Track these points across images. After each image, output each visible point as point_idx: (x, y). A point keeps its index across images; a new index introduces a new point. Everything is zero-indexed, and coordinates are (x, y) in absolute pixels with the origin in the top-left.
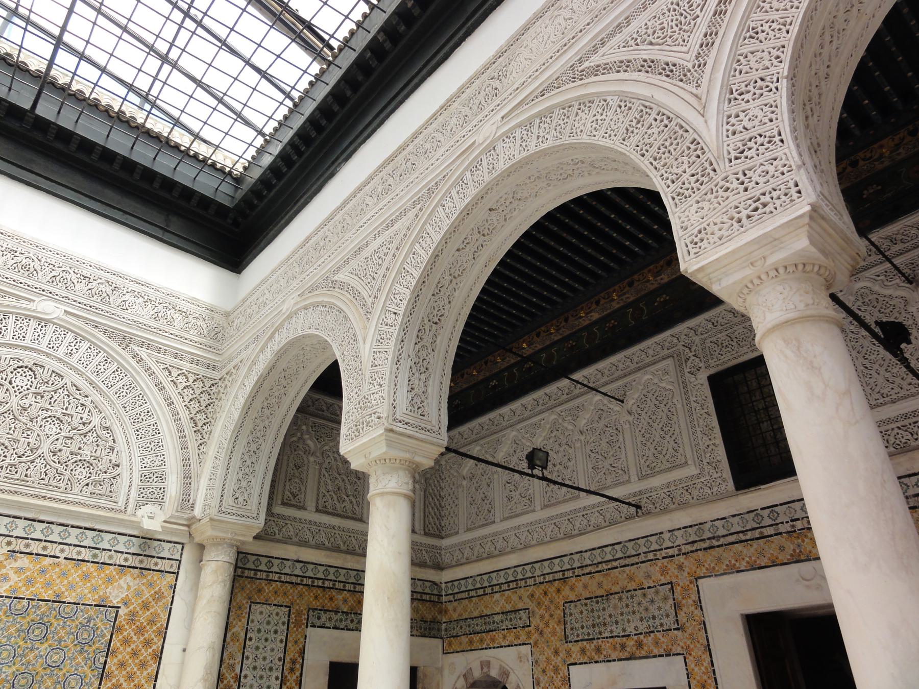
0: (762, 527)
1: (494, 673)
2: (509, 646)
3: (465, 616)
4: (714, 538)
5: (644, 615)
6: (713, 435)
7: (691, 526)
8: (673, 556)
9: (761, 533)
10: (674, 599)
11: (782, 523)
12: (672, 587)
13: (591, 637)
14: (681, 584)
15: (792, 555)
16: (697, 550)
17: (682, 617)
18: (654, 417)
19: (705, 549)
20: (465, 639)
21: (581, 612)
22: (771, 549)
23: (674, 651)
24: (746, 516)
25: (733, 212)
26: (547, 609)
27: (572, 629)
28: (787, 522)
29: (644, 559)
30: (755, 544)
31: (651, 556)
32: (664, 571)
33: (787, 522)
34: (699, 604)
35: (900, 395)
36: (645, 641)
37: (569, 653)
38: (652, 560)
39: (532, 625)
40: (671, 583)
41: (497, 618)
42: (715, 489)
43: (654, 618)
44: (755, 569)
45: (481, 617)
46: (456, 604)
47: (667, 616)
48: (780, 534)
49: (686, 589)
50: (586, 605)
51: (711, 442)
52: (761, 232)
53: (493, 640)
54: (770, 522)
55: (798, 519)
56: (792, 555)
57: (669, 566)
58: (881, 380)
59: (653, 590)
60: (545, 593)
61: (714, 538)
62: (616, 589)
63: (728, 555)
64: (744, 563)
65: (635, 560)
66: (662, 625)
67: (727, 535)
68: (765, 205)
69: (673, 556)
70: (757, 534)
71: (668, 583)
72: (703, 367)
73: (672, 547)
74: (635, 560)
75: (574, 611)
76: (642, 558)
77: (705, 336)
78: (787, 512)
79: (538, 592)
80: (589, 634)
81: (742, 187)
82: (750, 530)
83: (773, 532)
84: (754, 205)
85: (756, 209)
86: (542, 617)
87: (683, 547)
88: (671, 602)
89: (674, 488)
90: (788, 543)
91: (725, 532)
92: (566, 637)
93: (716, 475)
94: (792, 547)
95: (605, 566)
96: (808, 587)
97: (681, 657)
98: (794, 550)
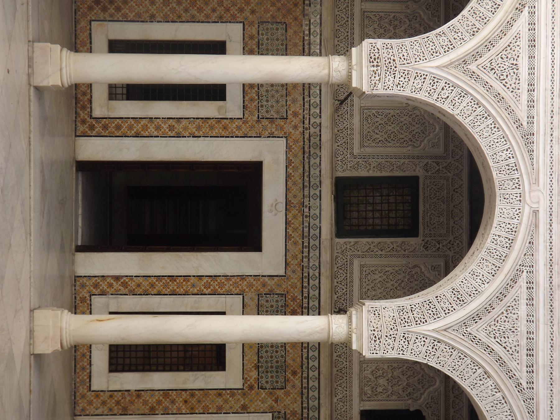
0: (310, 188)
4: (310, 155)
5: (270, 93)
6: (376, 170)
7: (320, 140)
8: (304, 124)
9: (306, 187)
10: (277, 118)
11: (309, 201)
12: (284, 119)
13: (260, 46)
14: (285, 126)
15: (291, 201)
16: (304, 142)
17: (265, 122)
18: (404, 128)
19: (304, 147)
21: (278, 40)
22: (295, 190)
23: (246, 112)
24: (318, 179)
25: (379, 329)
27: (267, 29)
28: (309, 204)
29: (306, 100)
30: (300, 181)
31: (307, 106)
32: (295, 114)
33: (309, 204)
34: (271, 136)
35: (364, 284)
36: (254, 91)
37: (251, 24)
38: (304, 106)
40: (287, 119)
42: (340, 163)
43: (267, 101)
44: (286, 178)
47: (267, 112)
48: (304, 198)
49: (282, 128)
50: (282, 45)
51: (372, 167)
52: (364, 337)
54: (311, 194)
55: (309, 210)
56: (291, 201)
57: (298, 119)
58: (376, 277)
59: (285, 103)
61: (310, 155)
63: (297, 162)
64: (291, 172)
65: (306, 93)
66: (262, 106)
67: (309, 164)
68: (375, 341)
69: (304, 124)
70: (306, 184)
71: (287, 116)
72: (427, 174)
73: (309, 124)
74: (306, 93)
75: (280, 32)
76: (307, 99)
77: (450, 181)
78: (315, 205)
80: (262, 45)
81: (388, 335)
82: (309, 180)
83: (305, 194)
84: (377, 337)
85: (375, 337)
87: (308, 131)
88: (276, 116)
89: (349, 133)
90: (297, 201)
91: (311, 163)
93: (349, 166)
94: (295, 202)
96: (272, 205)
97: (242, 117)
98: (293, 203)
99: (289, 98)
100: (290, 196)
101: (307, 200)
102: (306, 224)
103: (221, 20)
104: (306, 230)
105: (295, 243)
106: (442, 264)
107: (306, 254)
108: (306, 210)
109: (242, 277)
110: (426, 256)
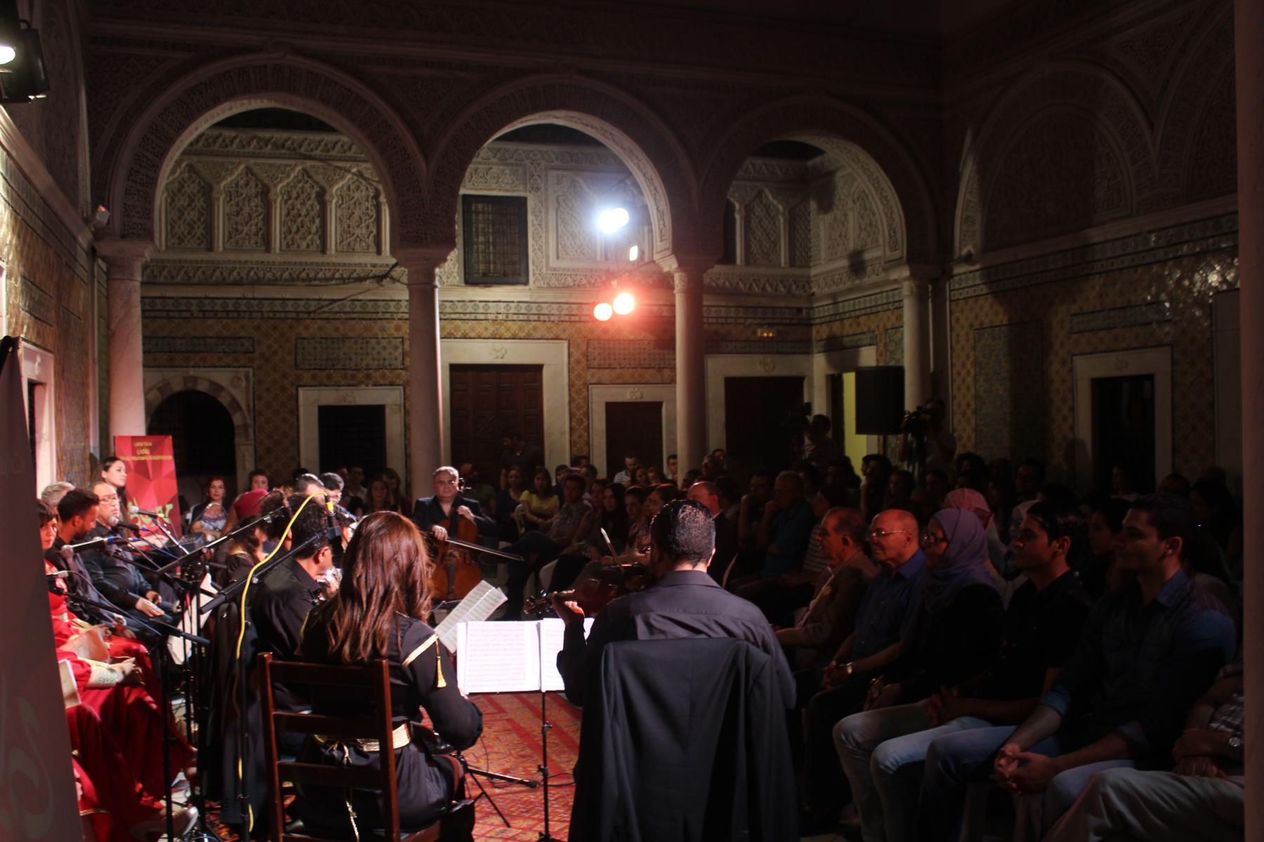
1: (202, 387)
30: (470, 323)
31: (388, 316)
41: (209, 341)
62: (350, 334)
65: (374, 316)
70: (473, 317)
76: (380, 315)
86: (269, 347)
92: (296, 365)
95: (343, 316)
99: (380, 336)
100: (486, 334)
101: (490, 317)
102: (515, 317)
103: (295, 412)
104: (521, 317)
105: (535, 328)
106: (555, 173)
107: (546, 318)
108: (500, 317)
109: (571, 385)
110: (546, 189)
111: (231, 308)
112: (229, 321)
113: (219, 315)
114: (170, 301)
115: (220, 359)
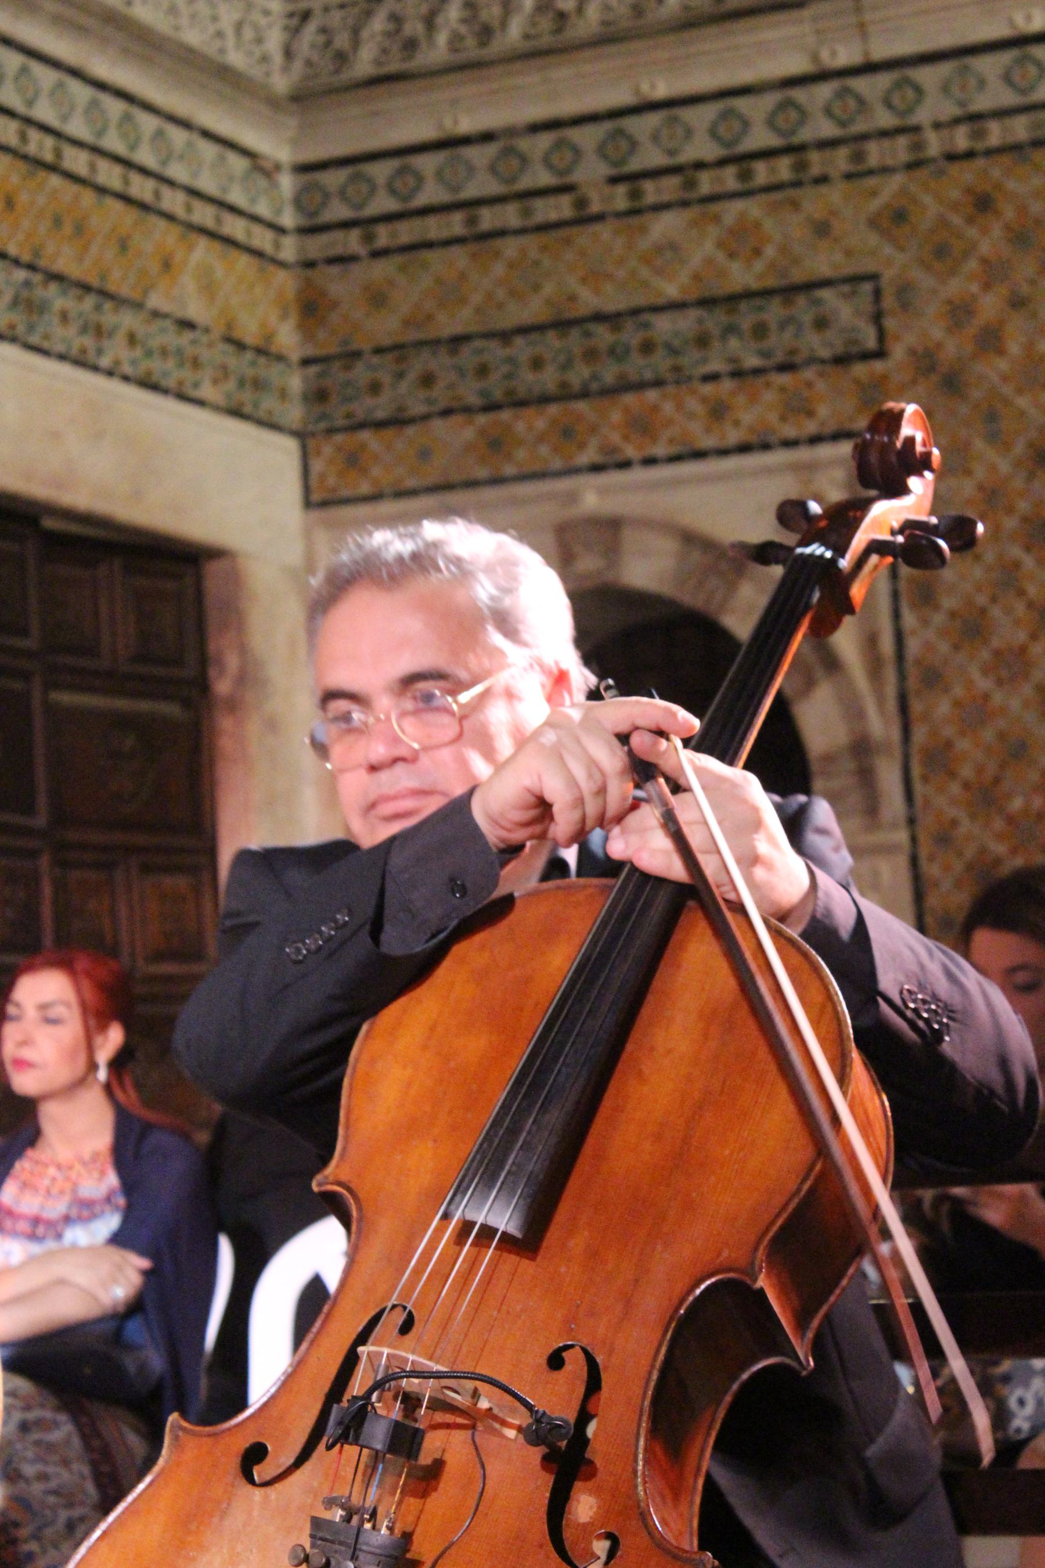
2: (744, 448)
3: (447, 325)
20: (455, 435)
26: (992, 273)
39: (898, 352)
41: (664, 325)
45: (562, 325)
46: (381, 270)
53: (643, 426)
60: (983, 204)
79: (934, 202)
86: (959, 313)
111: (760, 138)
112: (753, 208)
113: (706, 182)
114: (479, 155)
115: (718, 412)
